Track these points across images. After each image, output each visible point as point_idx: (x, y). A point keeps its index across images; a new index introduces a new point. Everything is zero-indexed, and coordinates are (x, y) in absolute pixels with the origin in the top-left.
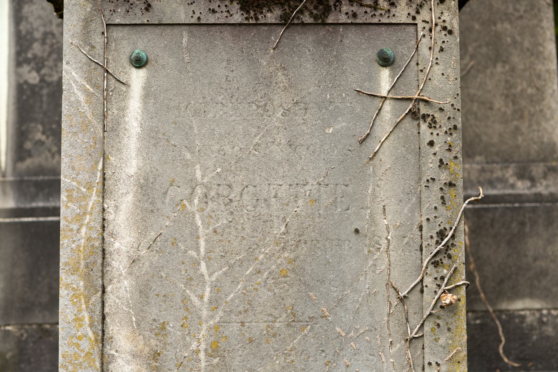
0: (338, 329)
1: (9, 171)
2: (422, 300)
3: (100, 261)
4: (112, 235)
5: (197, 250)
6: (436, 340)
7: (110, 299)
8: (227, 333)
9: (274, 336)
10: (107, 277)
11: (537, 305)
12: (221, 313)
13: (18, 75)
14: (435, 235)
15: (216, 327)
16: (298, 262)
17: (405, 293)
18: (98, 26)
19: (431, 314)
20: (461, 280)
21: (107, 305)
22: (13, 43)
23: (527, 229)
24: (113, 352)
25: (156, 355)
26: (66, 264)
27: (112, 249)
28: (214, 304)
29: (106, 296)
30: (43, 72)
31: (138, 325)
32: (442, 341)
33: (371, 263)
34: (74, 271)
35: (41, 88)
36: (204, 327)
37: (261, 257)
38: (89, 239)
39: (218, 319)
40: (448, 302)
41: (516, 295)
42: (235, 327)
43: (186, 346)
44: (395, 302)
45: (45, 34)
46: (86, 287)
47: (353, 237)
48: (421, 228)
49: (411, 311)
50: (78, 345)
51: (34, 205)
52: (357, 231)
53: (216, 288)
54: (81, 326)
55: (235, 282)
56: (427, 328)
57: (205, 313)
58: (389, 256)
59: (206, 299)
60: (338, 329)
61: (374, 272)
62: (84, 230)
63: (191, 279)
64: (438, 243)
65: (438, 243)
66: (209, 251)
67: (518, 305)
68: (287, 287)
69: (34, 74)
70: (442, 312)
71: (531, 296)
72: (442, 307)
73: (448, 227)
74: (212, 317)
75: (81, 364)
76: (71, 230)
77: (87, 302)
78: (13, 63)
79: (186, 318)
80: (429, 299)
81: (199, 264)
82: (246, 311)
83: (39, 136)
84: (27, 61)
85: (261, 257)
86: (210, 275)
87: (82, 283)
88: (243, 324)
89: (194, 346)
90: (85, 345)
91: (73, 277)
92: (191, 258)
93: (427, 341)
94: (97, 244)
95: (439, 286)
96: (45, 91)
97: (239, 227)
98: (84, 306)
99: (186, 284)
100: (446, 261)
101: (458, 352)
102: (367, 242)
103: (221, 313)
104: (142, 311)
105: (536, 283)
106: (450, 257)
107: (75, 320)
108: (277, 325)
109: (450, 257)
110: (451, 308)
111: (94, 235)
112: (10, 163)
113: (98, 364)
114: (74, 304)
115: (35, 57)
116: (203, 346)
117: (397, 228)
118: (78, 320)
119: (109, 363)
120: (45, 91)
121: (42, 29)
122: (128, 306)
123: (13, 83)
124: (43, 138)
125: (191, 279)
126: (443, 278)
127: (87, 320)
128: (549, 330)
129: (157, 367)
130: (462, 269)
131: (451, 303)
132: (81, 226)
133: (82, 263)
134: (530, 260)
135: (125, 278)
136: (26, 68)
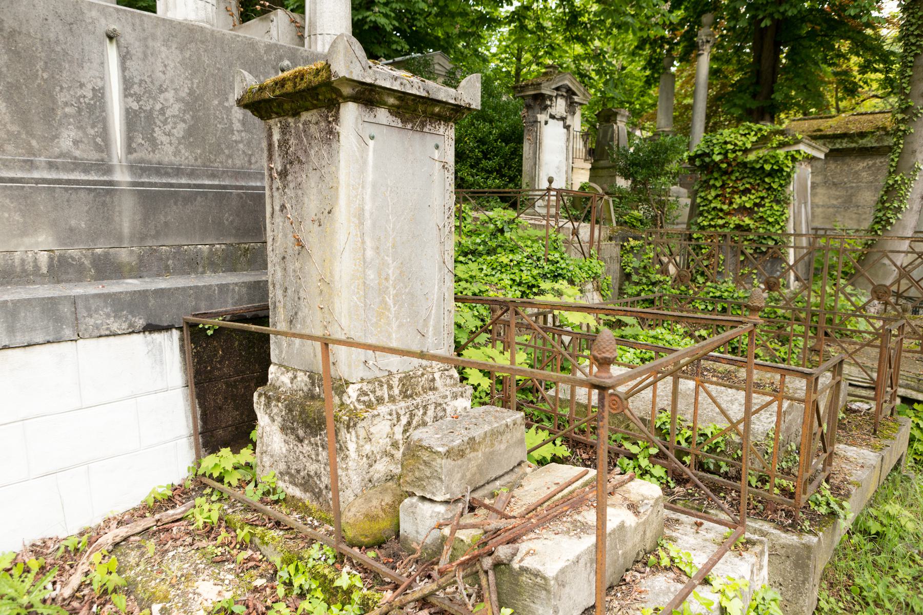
1: (124, 160)
13: (126, 103)
18: (360, 121)
22: (121, 83)
25: (378, 248)
28: (393, 229)
30: (141, 103)
35: (140, 113)
45: (141, 81)
51: (143, 180)
69: (135, 104)
78: (122, 95)
83: (140, 141)
84: (131, 95)
96: (142, 115)
112: (124, 155)
115: (135, 94)
120: (142, 115)
121: (139, 77)
123: (123, 107)
124: (143, 142)
136: (130, 99)
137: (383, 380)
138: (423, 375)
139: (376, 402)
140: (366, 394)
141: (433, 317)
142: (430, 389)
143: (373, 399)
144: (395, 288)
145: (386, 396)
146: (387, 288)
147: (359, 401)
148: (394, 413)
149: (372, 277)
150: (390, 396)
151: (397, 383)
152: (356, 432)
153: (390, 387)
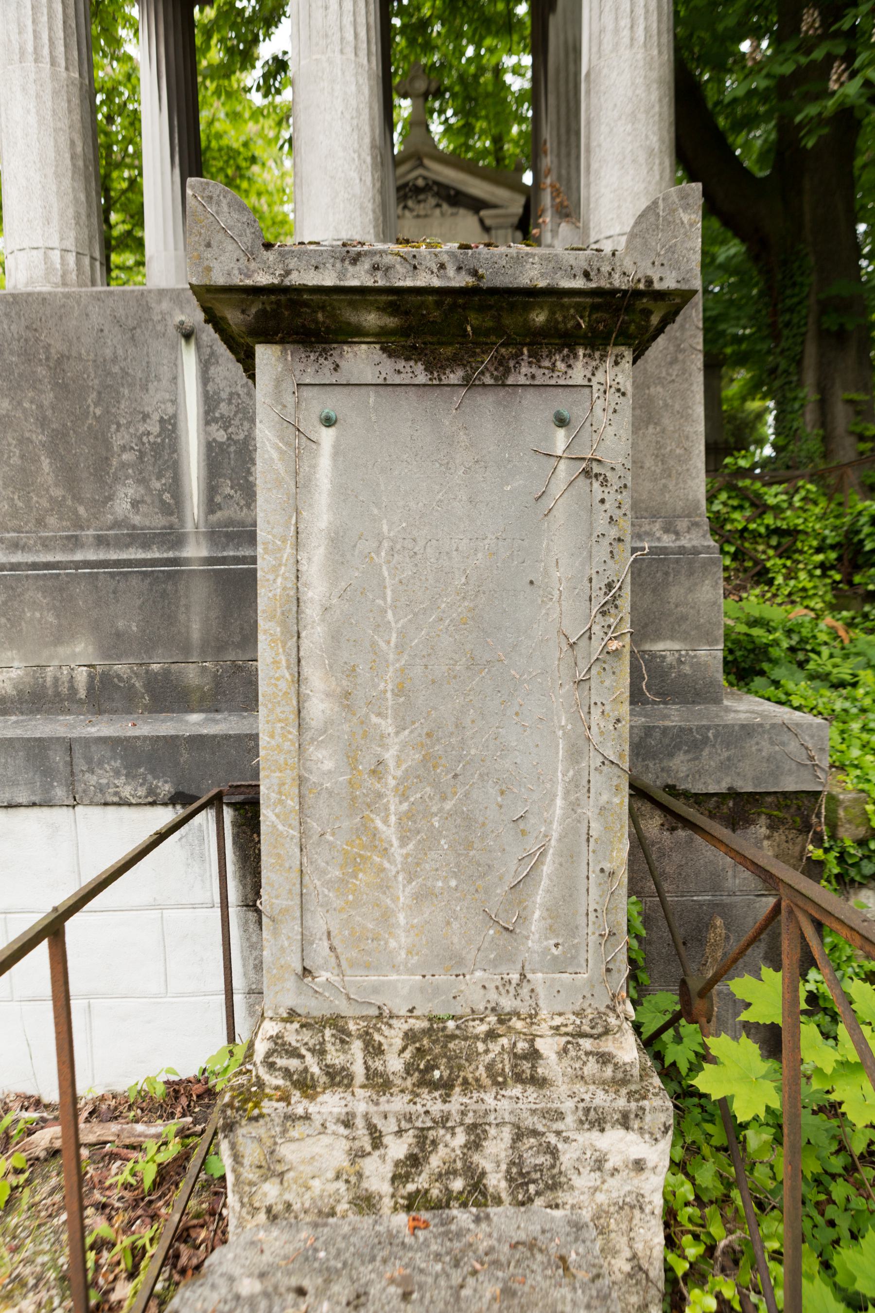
0: (513, 672)
1: (202, 523)
2: (590, 646)
3: (295, 609)
4: (305, 585)
5: (384, 598)
6: (602, 682)
7: (305, 643)
8: (411, 675)
9: (455, 677)
10: (301, 624)
11: (677, 647)
12: (406, 657)
13: (207, 433)
14: (603, 587)
15: (402, 670)
16: (477, 611)
17: (574, 640)
18: (289, 386)
19: (597, 659)
20: (626, 628)
21: (301, 649)
22: (201, 403)
23: (671, 579)
24: (308, 692)
25: (347, 695)
26: (264, 611)
27: (305, 598)
28: (400, 649)
29: (301, 641)
30: (230, 430)
31: (331, 667)
32: (607, 683)
33: (544, 611)
34: (272, 618)
35: (229, 446)
36: (391, 669)
37: (443, 605)
38: (284, 589)
39: (403, 662)
40: (614, 648)
41: (658, 636)
42: (419, 670)
43: (375, 686)
44: (565, 648)
45: (231, 394)
46: (282, 633)
47: (528, 588)
48: (591, 580)
49: (579, 656)
50: (276, 685)
51: (225, 554)
52: (532, 582)
53: (402, 634)
54: (278, 668)
55: (419, 629)
56: (594, 671)
57: (391, 657)
58: (560, 605)
59: (392, 644)
60: (513, 672)
61: (547, 620)
62: (279, 580)
63: (379, 626)
64: (606, 594)
65: (606, 594)
66: (395, 600)
67: (659, 646)
68: (466, 633)
69: (222, 432)
70: (608, 657)
71: (672, 638)
72: (608, 653)
73: (615, 580)
74: (398, 660)
75: (279, 702)
76: (268, 580)
77: (283, 647)
78: (202, 422)
79: (374, 661)
80: (597, 645)
81: (386, 612)
82: (429, 655)
83: (228, 491)
84: (215, 420)
85: (443, 605)
86: (396, 622)
87: (278, 629)
88: (426, 666)
89: (382, 686)
90: (283, 685)
91: (270, 624)
92: (379, 606)
93: (593, 683)
94: (292, 593)
95: (606, 633)
96: (232, 449)
97: (423, 578)
98: (281, 650)
99: (374, 631)
100: (612, 611)
101: (622, 693)
102: (541, 592)
103: (406, 657)
104: (334, 654)
105: (677, 627)
106: (616, 607)
107: (273, 663)
108: (458, 668)
109: (616, 607)
110: (616, 653)
111: (290, 585)
112: (202, 514)
113: (295, 703)
114: (272, 648)
115: (222, 416)
116: (390, 687)
117: (569, 580)
118: (276, 662)
119: (305, 701)
120: (232, 449)
121: (228, 390)
122: (321, 650)
123: (203, 441)
124: (232, 492)
125: (379, 626)
126: (609, 626)
127: (284, 663)
128: (687, 669)
129: (348, 705)
130: (628, 619)
131: (617, 649)
132: (277, 576)
133: (279, 611)
134: (673, 606)
135: (319, 624)
136: (214, 427)
137: (352, 1027)
138: (491, 1035)
139: (324, 1079)
140: (294, 1053)
141: (545, 883)
142: (519, 1078)
143: (315, 1069)
144: (404, 797)
145: (358, 1070)
146: (380, 796)
147: (271, 1066)
148: (360, 1122)
149: (328, 765)
150: (371, 1075)
151: (398, 1043)
152: (233, 1146)
153: (374, 1050)
